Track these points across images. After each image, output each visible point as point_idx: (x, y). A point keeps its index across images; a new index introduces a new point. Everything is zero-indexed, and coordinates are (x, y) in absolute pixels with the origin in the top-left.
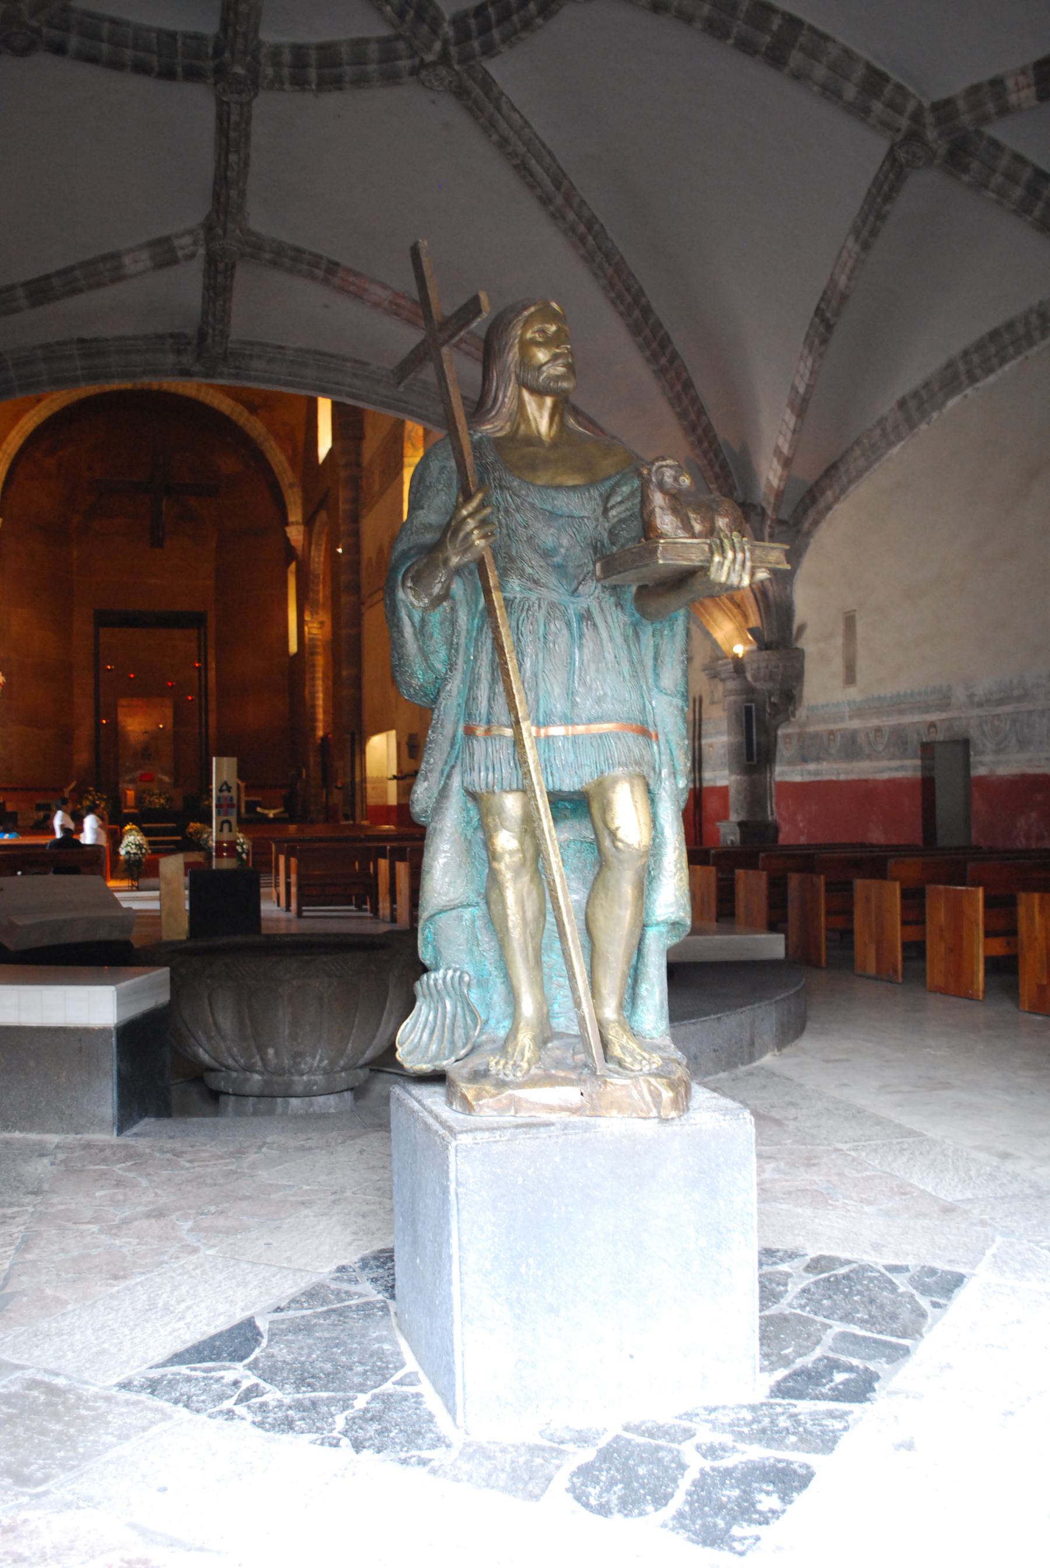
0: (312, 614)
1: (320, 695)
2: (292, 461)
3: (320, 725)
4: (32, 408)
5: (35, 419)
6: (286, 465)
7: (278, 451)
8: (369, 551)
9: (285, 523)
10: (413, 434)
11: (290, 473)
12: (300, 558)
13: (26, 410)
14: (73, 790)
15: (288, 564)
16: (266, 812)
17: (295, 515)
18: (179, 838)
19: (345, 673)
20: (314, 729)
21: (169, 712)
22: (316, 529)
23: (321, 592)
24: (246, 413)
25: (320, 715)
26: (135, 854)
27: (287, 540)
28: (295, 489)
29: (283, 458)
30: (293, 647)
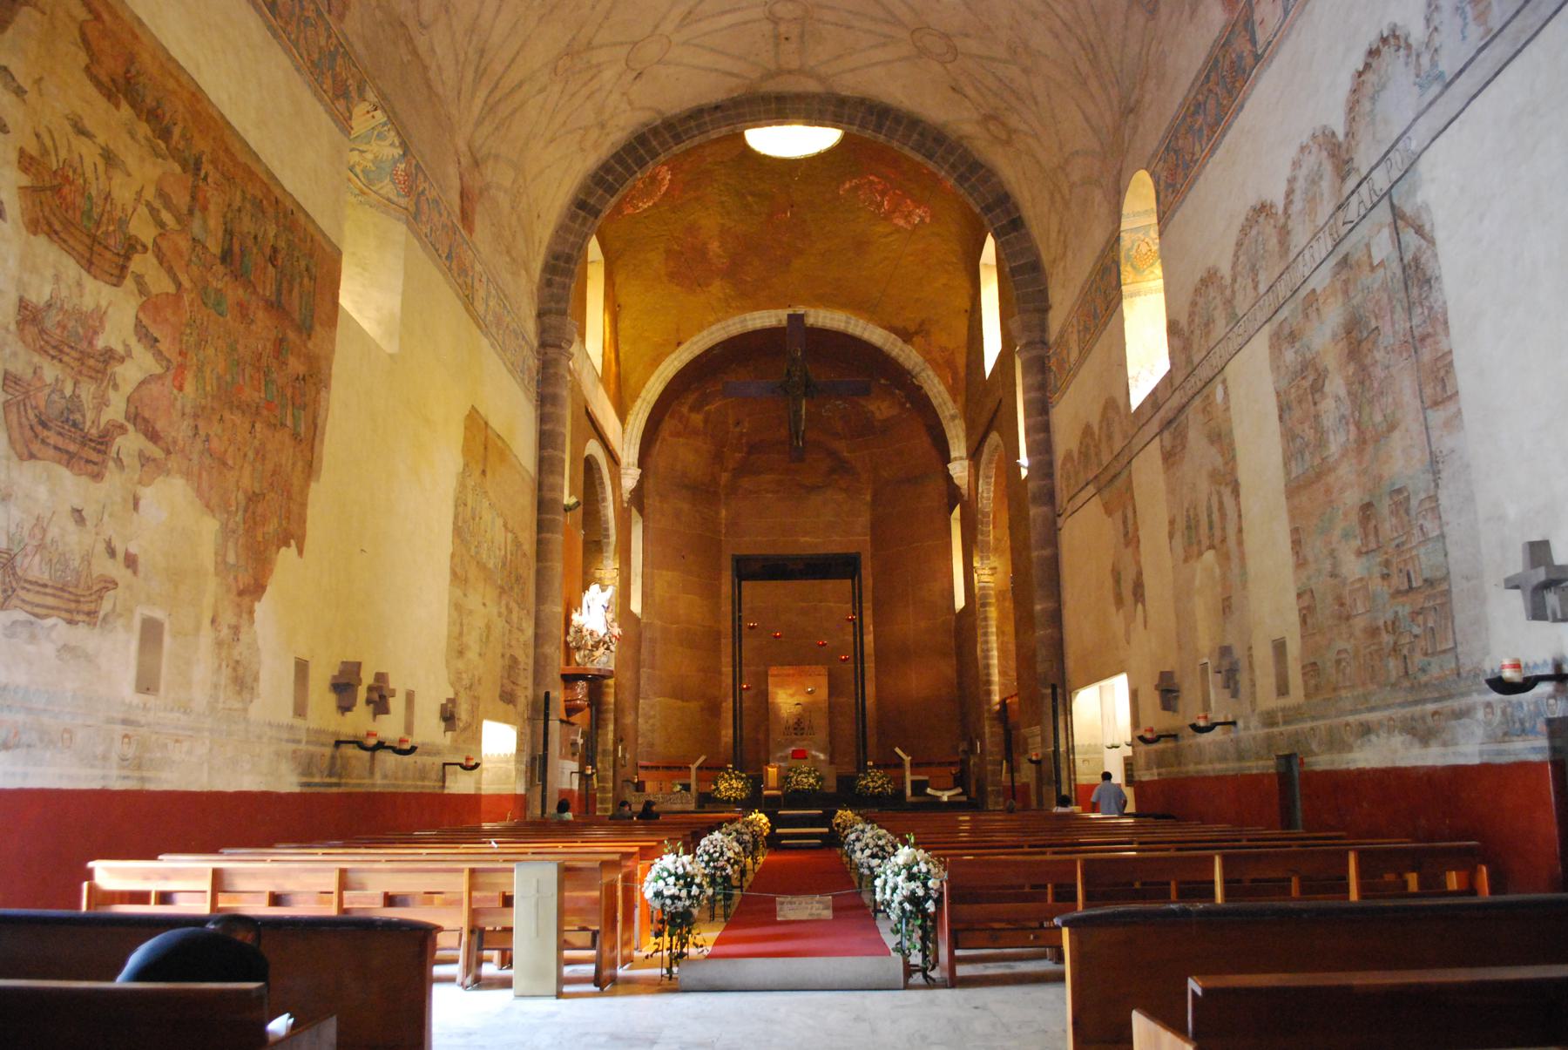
0: (982, 558)
1: (995, 653)
2: (953, 391)
3: (996, 688)
4: (673, 352)
5: (676, 363)
6: (946, 396)
7: (936, 380)
8: (1065, 440)
9: (946, 459)
10: (1133, 253)
11: (950, 404)
12: (966, 498)
13: (667, 355)
14: (700, 768)
15: (951, 513)
16: (939, 793)
17: (958, 448)
18: (826, 830)
19: (1038, 607)
20: (989, 693)
21: (824, 681)
22: (985, 457)
23: (994, 532)
24: (900, 342)
25: (996, 677)
26: (673, 897)
27: (949, 478)
28: (957, 421)
29: (942, 388)
30: (960, 602)
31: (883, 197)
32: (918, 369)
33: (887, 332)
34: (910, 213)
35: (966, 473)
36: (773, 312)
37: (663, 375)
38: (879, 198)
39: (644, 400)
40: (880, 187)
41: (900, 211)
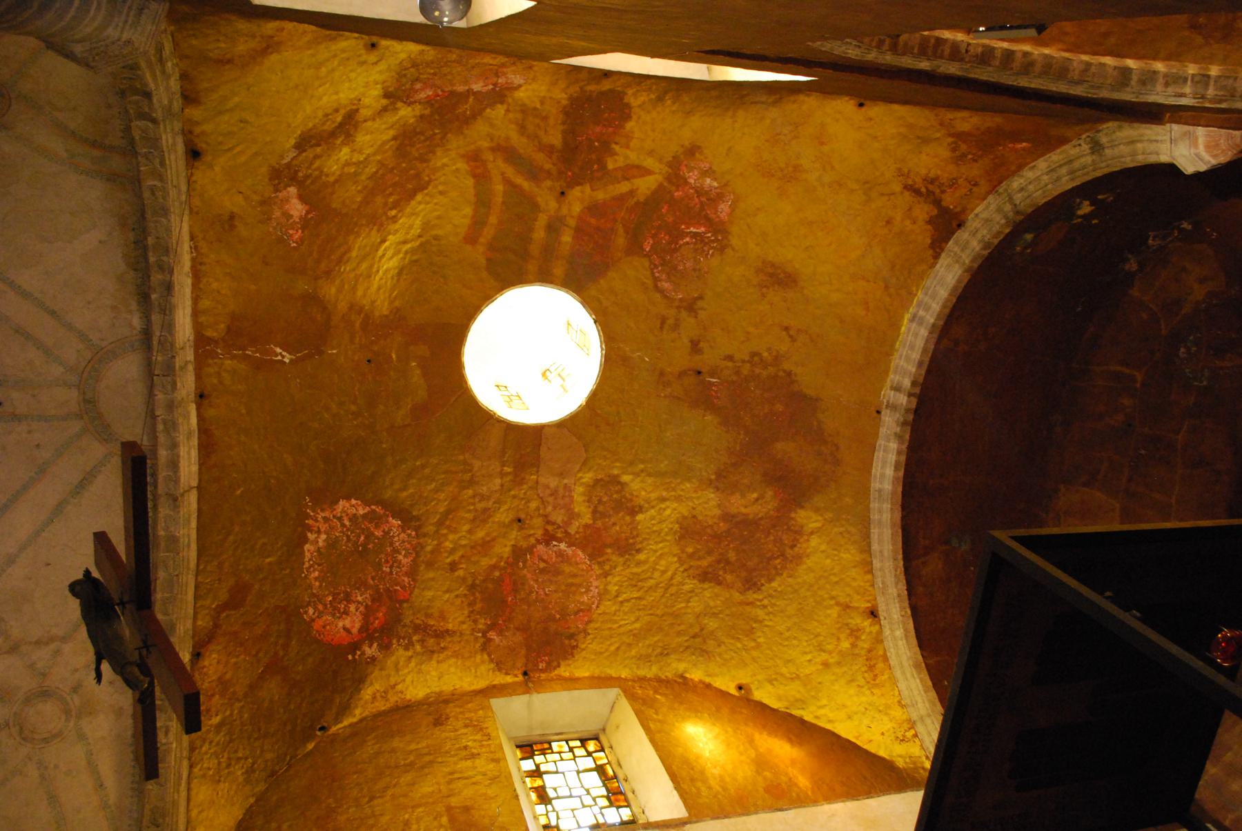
2: (1046, 144)
6: (1056, 157)
7: (1029, 174)
11: (1070, 150)
24: (962, 235)
28: (1104, 140)
29: (1042, 164)
31: (683, 235)
32: (1008, 207)
33: (943, 255)
34: (699, 192)
35: (1201, 131)
36: (881, 442)
37: (906, 664)
38: (687, 239)
39: (922, 718)
40: (664, 238)
41: (702, 208)
